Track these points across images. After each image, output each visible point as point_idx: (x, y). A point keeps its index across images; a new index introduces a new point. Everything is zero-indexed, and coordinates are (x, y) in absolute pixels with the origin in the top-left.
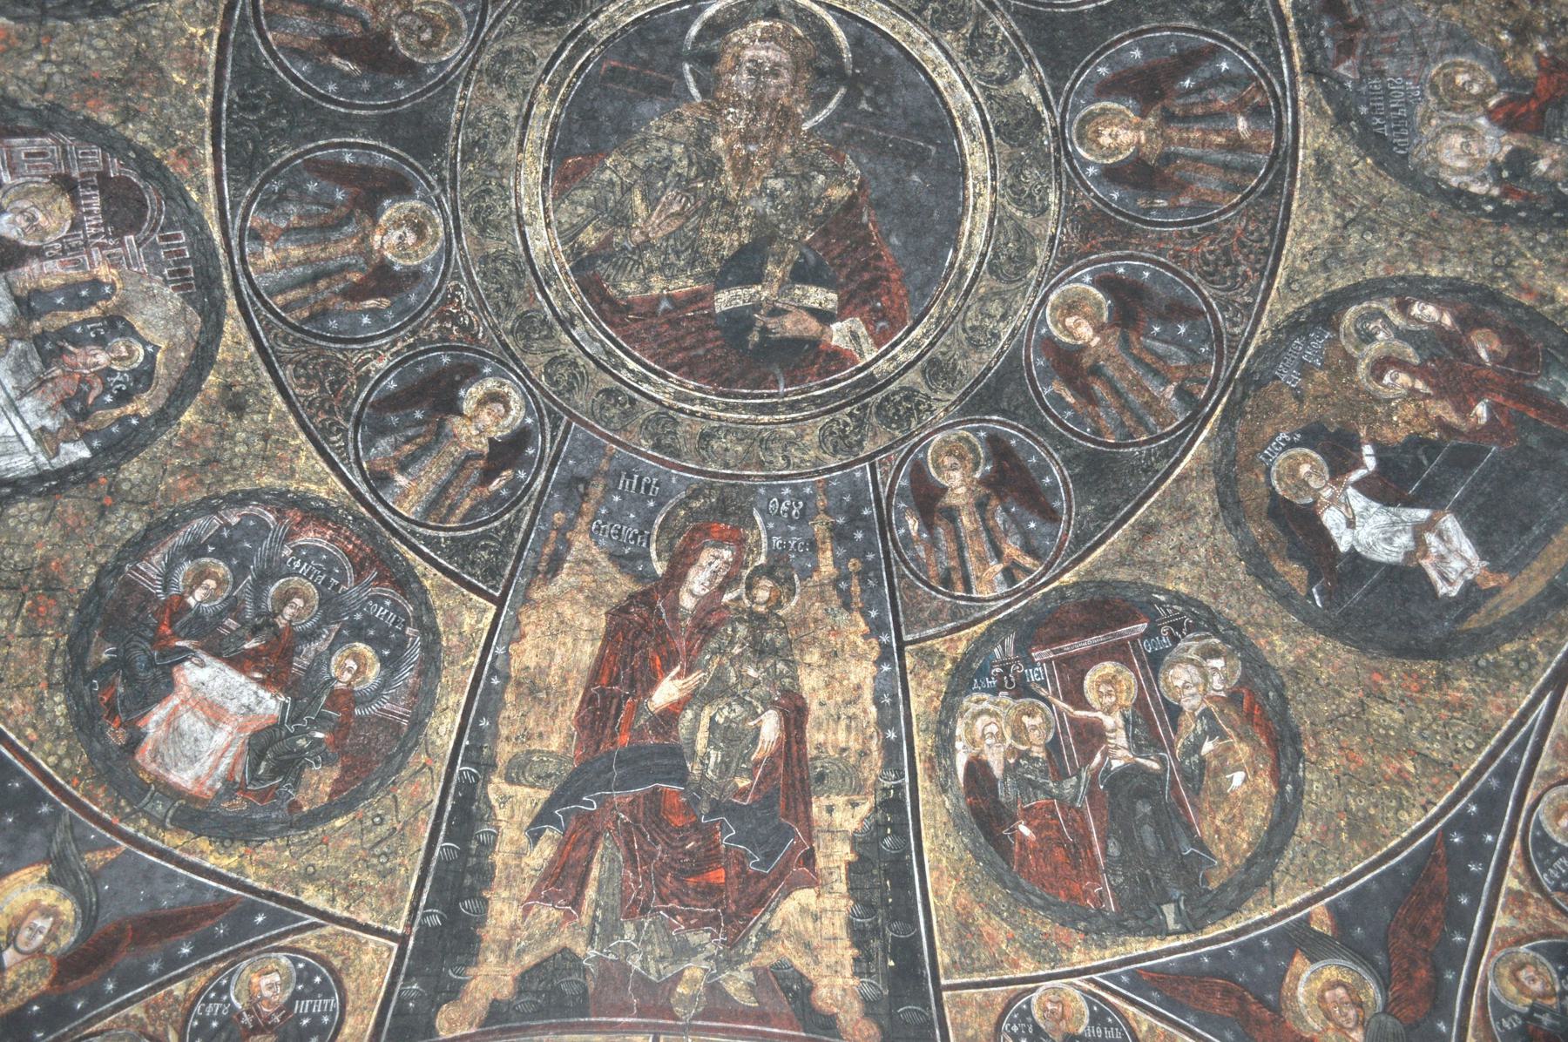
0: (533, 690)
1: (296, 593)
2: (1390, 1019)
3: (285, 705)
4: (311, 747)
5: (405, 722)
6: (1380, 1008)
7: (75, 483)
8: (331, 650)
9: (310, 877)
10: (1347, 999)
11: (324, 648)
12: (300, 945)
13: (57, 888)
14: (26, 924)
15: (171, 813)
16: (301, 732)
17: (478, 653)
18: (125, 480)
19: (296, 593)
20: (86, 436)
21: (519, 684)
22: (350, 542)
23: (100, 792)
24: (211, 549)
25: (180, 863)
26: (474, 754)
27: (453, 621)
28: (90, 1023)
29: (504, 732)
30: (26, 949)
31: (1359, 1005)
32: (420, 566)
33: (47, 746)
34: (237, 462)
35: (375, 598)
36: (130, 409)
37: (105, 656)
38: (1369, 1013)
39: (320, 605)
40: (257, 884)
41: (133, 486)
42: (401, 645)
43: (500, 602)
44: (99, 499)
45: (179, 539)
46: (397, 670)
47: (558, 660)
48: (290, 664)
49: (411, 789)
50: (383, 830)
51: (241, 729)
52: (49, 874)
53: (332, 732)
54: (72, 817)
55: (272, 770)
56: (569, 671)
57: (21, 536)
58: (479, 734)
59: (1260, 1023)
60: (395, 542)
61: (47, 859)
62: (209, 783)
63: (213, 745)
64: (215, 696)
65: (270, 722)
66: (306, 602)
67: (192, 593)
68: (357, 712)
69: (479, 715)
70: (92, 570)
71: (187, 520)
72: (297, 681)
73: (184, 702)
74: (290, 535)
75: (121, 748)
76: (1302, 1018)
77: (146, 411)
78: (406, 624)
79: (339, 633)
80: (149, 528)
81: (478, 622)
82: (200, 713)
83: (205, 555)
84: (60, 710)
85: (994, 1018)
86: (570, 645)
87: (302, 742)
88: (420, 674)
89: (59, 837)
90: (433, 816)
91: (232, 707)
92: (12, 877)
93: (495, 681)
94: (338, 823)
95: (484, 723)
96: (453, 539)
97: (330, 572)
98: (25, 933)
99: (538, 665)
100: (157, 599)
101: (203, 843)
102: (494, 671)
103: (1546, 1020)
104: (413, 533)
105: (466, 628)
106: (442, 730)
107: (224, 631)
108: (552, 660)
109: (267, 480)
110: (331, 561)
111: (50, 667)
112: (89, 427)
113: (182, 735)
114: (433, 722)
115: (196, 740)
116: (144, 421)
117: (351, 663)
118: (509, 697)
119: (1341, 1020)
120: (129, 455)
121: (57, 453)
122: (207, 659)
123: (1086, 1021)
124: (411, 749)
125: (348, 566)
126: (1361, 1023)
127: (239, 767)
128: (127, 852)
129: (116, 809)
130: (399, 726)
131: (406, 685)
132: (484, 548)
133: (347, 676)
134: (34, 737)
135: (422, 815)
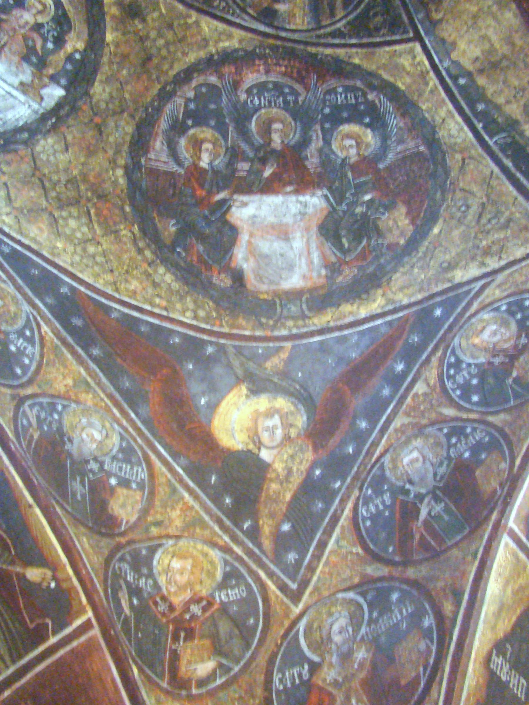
0: (495, 66)
1: (270, 121)
3: (326, 196)
4: (368, 208)
5: (422, 148)
7: (67, 116)
8: (327, 142)
9: (451, 266)
11: (321, 143)
12: (487, 301)
14: (260, 429)
15: (304, 306)
16: (353, 204)
17: (432, 74)
18: (98, 101)
19: (270, 121)
20: (54, 79)
21: (481, 71)
22: (280, 66)
23: (241, 321)
24: (190, 123)
25: (340, 328)
26: (493, 126)
27: (398, 69)
28: (369, 453)
29: (501, 100)
30: (275, 444)
32: (341, 52)
33: (178, 306)
34: (164, 52)
35: (329, 92)
36: (69, 48)
37: (173, 229)
39: (295, 120)
40: (413, 300)
41: (107, 103)
42: (372, 109)
43: (418, 38)
44: (92, 121)
45: (163, 124)
46: (384, 125)
47: (494, 38)
48: (305, 168)
49: (468, 177)
50: (474, 209)
51: (307, 230)
52: (249, 389)
53: (374, 188)
54: (235, 347)
55: (354, 239)
56: (510, 37)
57: (57, 166)
58: (482, 116)
60: (313, 50)
61: (239, 381)
62: (315, 274)
63: (297, 252)
64: (272, 219)
65: (325, 213)
66: (282, 122)
67: (200, 158)
68: (381, 166)
69: (472, 105)
70: (120, 172)
71: (159, 110)
72: (320, 176)
73: (251, 235)
74: (236, 85)
75: (232, 287)
77: (80, 46)
78: (365, 95)
79: (322, 128)
80: (139, 127)
81: (414, 57)
82: (269, 237)
83: (189, 128)
84: (169, 278)
86: (493, 23)
87: (359, 210)
88: (403, 115)
89: (236, 363)
90: (503, 178)
91: (289, 220)
92: (224, 404)
93: (462, 81)
94: (436, 230)
95: (480, 107)
96: (349, 23)
97: (282, 94)
98: (265, 437)
99: (483, 52)
100: (179, 175)
101: (346, 308)
102: (455, 79)
104: (319, 37)
105: (408, 68)
106: (454, 132)
107: (242, 174)
108: (490, 41)
109: (192, 57)
110: (277, 86)
111: (140, 251)
112: (51, 71)
113: (267, 256)
114: (442, 134)
115: (282, 255)
116: (84, 53)
117: (348, 142)
118: (481, 81)
120: (90, 82)
121: (42, 99)
122: (245, 198)
124: (444, 159)
125: (290, 82)
127: (328, 252)
128: (293, 347)
129: (261, 325)
130: (420, 154)
131: (400, 129)
132: (376, 15)
133: (353, 152)
134: (164, 303)
135: (494, 183)
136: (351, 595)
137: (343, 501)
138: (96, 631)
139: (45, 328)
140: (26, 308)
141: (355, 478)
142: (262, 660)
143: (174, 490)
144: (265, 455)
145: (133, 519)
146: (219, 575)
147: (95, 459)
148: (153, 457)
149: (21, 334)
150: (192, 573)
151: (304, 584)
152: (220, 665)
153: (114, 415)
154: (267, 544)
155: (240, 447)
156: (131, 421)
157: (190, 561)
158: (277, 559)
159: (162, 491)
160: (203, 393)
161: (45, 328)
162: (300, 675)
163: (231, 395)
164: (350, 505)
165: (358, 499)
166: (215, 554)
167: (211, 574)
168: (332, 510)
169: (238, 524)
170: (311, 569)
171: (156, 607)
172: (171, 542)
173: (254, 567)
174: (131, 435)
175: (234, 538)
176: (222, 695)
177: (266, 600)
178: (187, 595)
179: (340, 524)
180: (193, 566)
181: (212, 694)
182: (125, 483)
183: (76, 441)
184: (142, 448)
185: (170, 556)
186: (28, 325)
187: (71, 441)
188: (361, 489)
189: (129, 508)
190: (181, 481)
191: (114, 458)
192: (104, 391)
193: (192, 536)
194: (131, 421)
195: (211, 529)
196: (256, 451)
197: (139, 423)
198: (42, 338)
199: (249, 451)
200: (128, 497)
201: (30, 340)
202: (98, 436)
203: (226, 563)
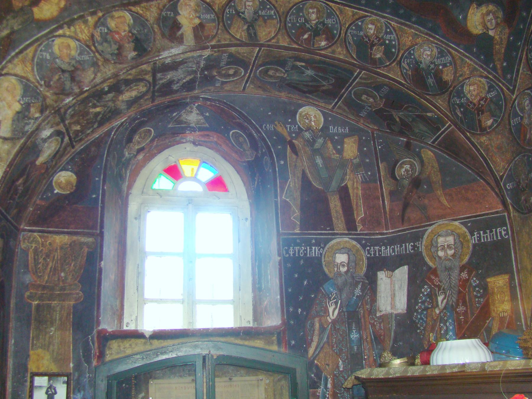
13: (483, 6)
14: (486, 22)
30: (493, 27)
52: (477, 5)
92: (469, 15)
98: (489, 24)
136: (529, 91)
137: (522, 51)
138: (453, 127)
139: (393, 23)
140: (383, 20)
141: (525, 40)
142: (506, 116)
143: (462, 60)
144: (491, 33)
145: (452, 78)
146: (487, 88)
147: (432, 63)
148: (451, 50)
149: (386, 33)
150: (478, 90)
151: (515, 87)
152: (494, 120)
153: (430, 40)
154: (500, 72)
155: (481, 32)
156: (437, 39)
157: (476, 85)
158: (504, 77)
159: (458, 62)
160: (460, 14)
161: (393, 23)
162: (518, 120)
163: (470, 10)
164: (525, 53)
165: (527, 49)
166: (483, 80)
167: (484, 88)
168: (519, 55)
169: (488, 66)
170: (516, 81)
171: (469, 107)
172: (467, 81)
173: (497, 82)
174: (439, 45)
175: (488, 72)
176: (497, 130)
177: (504, 94)
178: (478, 98)
179: (523, 61)
180: (477, 87)
181: (494, 130)
182: (445, 66)
183: (423, 62)
184: (446, 49)
185: (469, 86)
186: (387, 27)
187: (421, 63)
188: (528, 46)
189: (450, 74)
190: (464, 55)
191: (438, 58)
192: (423, 34)
193: (474, 76)
194: (437, 39)
195: (479, 70)
196: (487, 32)
197: (441, 39)
198: (394, 28)
199: (484, 33)
200: (447, 70)
201: (391, 33)
202: (429, 53)
203: (488, 83)
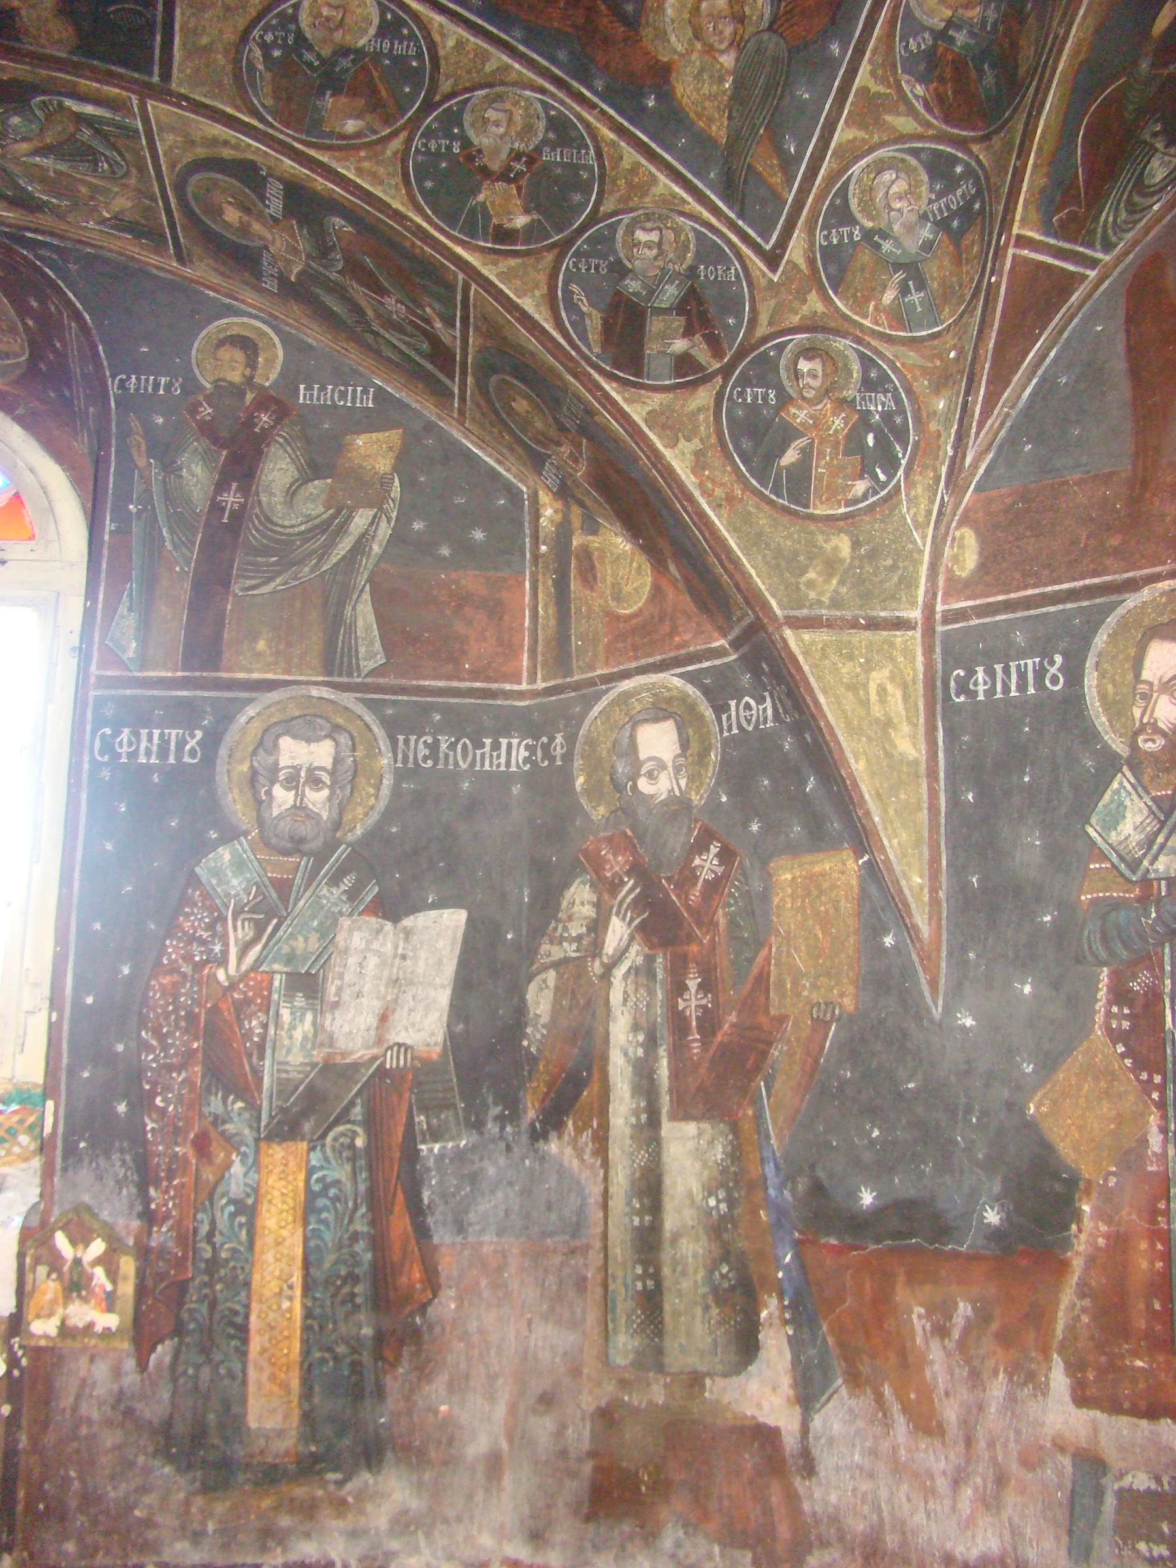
2: (775, 38)
6: (765, 24)
10: (727, 12)
31: (740, 19)
38: (751, 29)
59: (606, 41)
76: (662, 35)
85: (242, 23)
103: (961, 38)
119: (714, 40)
123: (372, 31)
126: (737, 43)
